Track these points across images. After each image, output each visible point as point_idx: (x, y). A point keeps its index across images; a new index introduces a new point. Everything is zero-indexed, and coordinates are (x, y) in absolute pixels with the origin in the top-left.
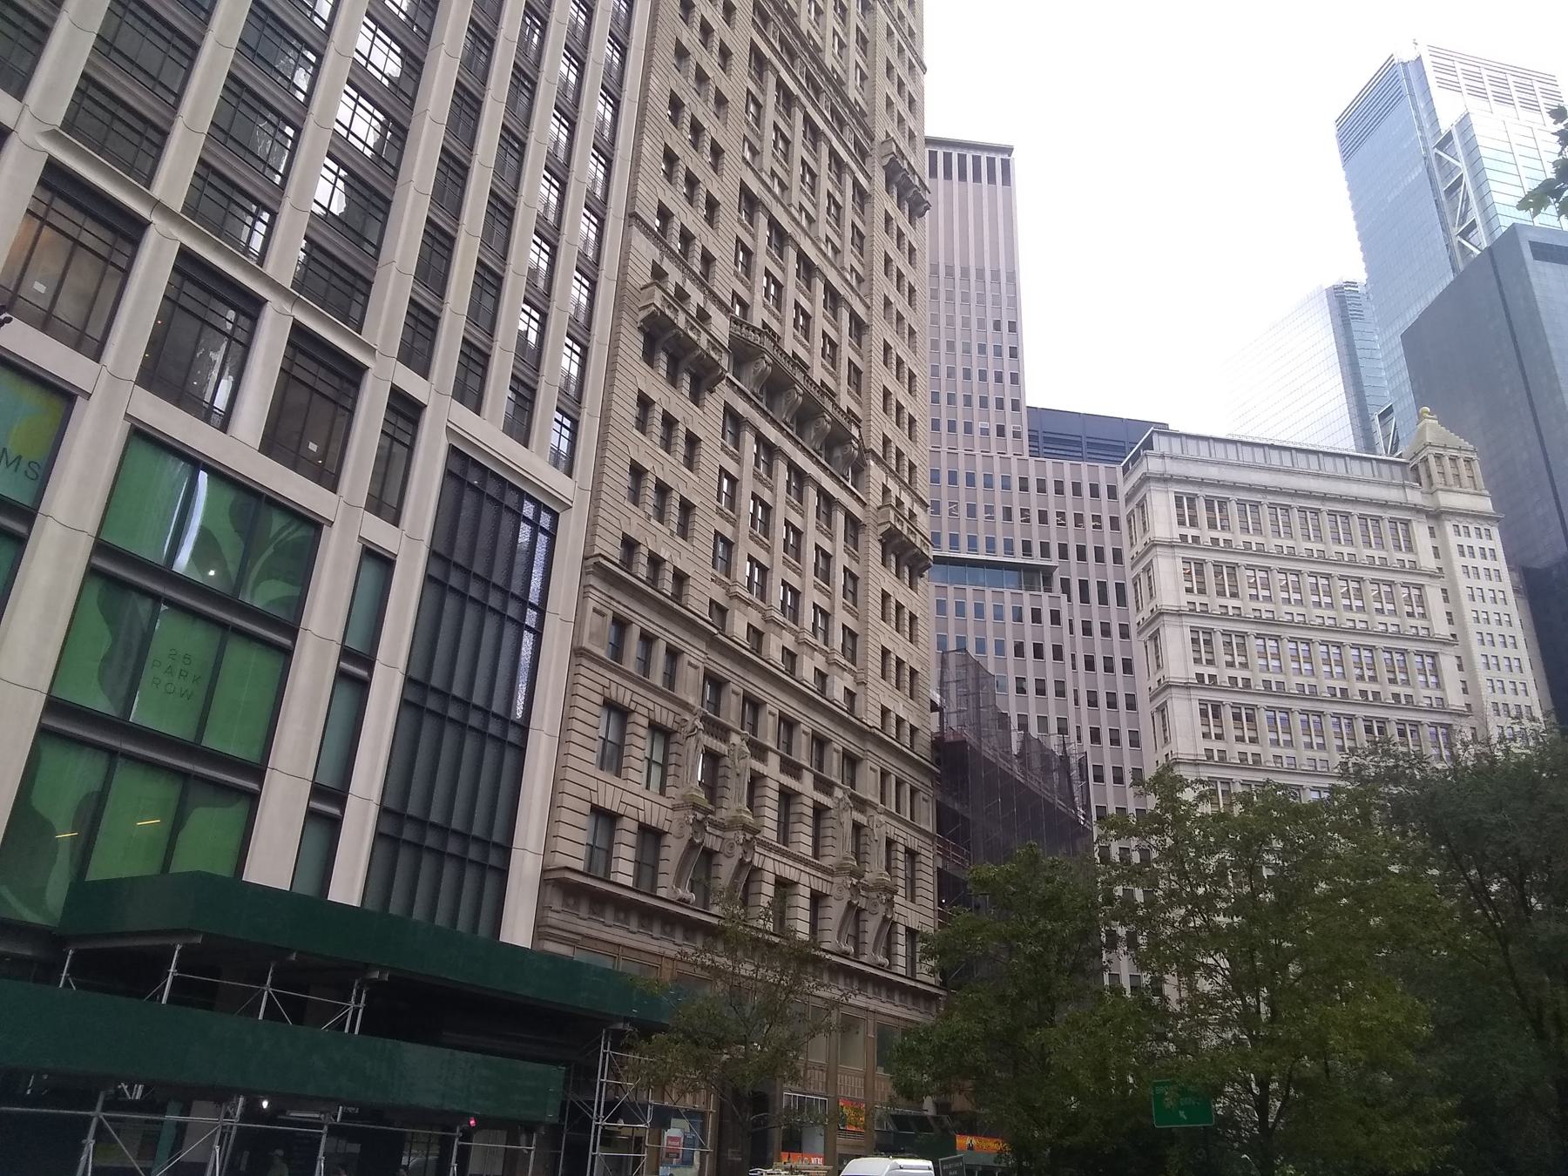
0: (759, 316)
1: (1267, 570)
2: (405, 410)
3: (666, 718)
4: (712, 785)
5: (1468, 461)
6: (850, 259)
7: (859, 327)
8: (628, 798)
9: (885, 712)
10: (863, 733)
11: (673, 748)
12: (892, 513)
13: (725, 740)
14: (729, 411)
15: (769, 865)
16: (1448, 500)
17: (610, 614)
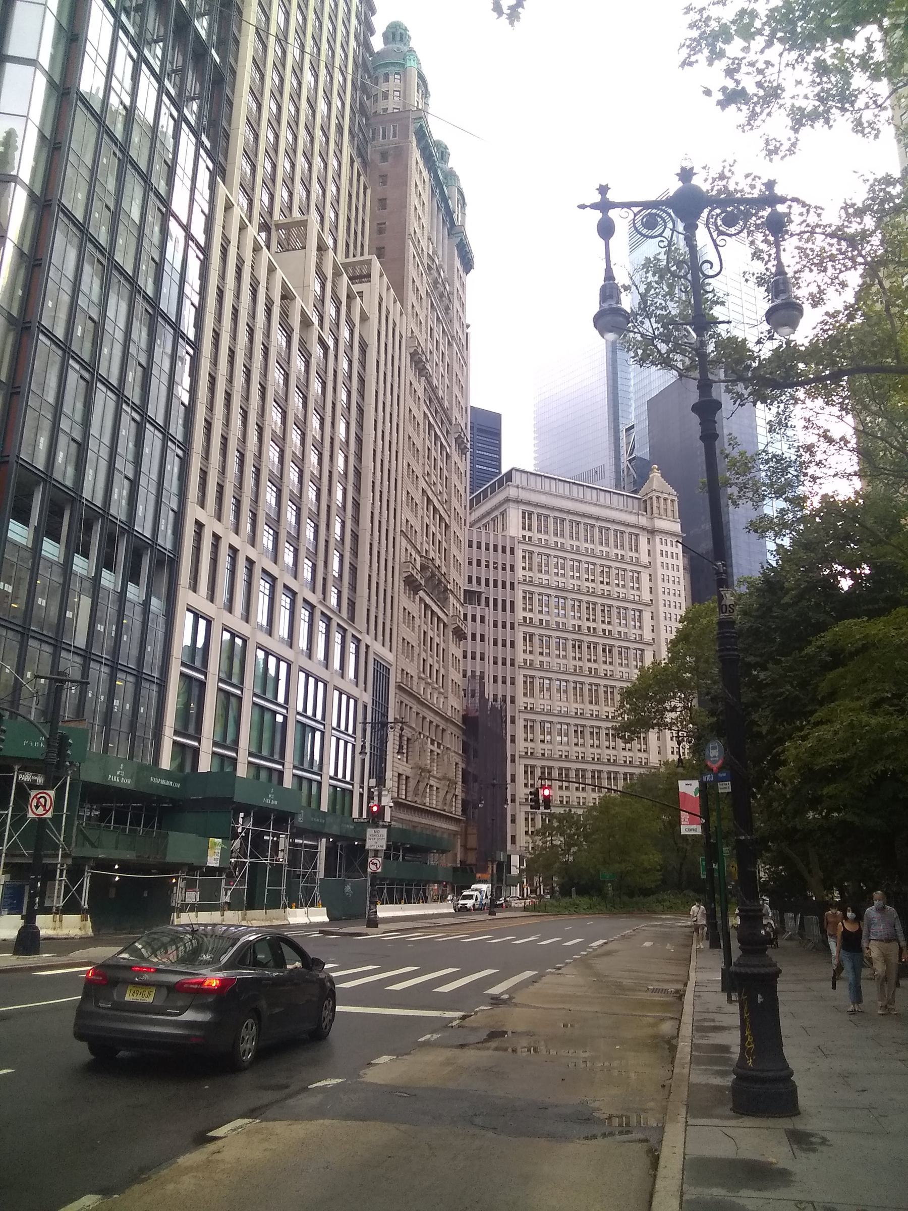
5: (672, 501)
16: (661, 524)
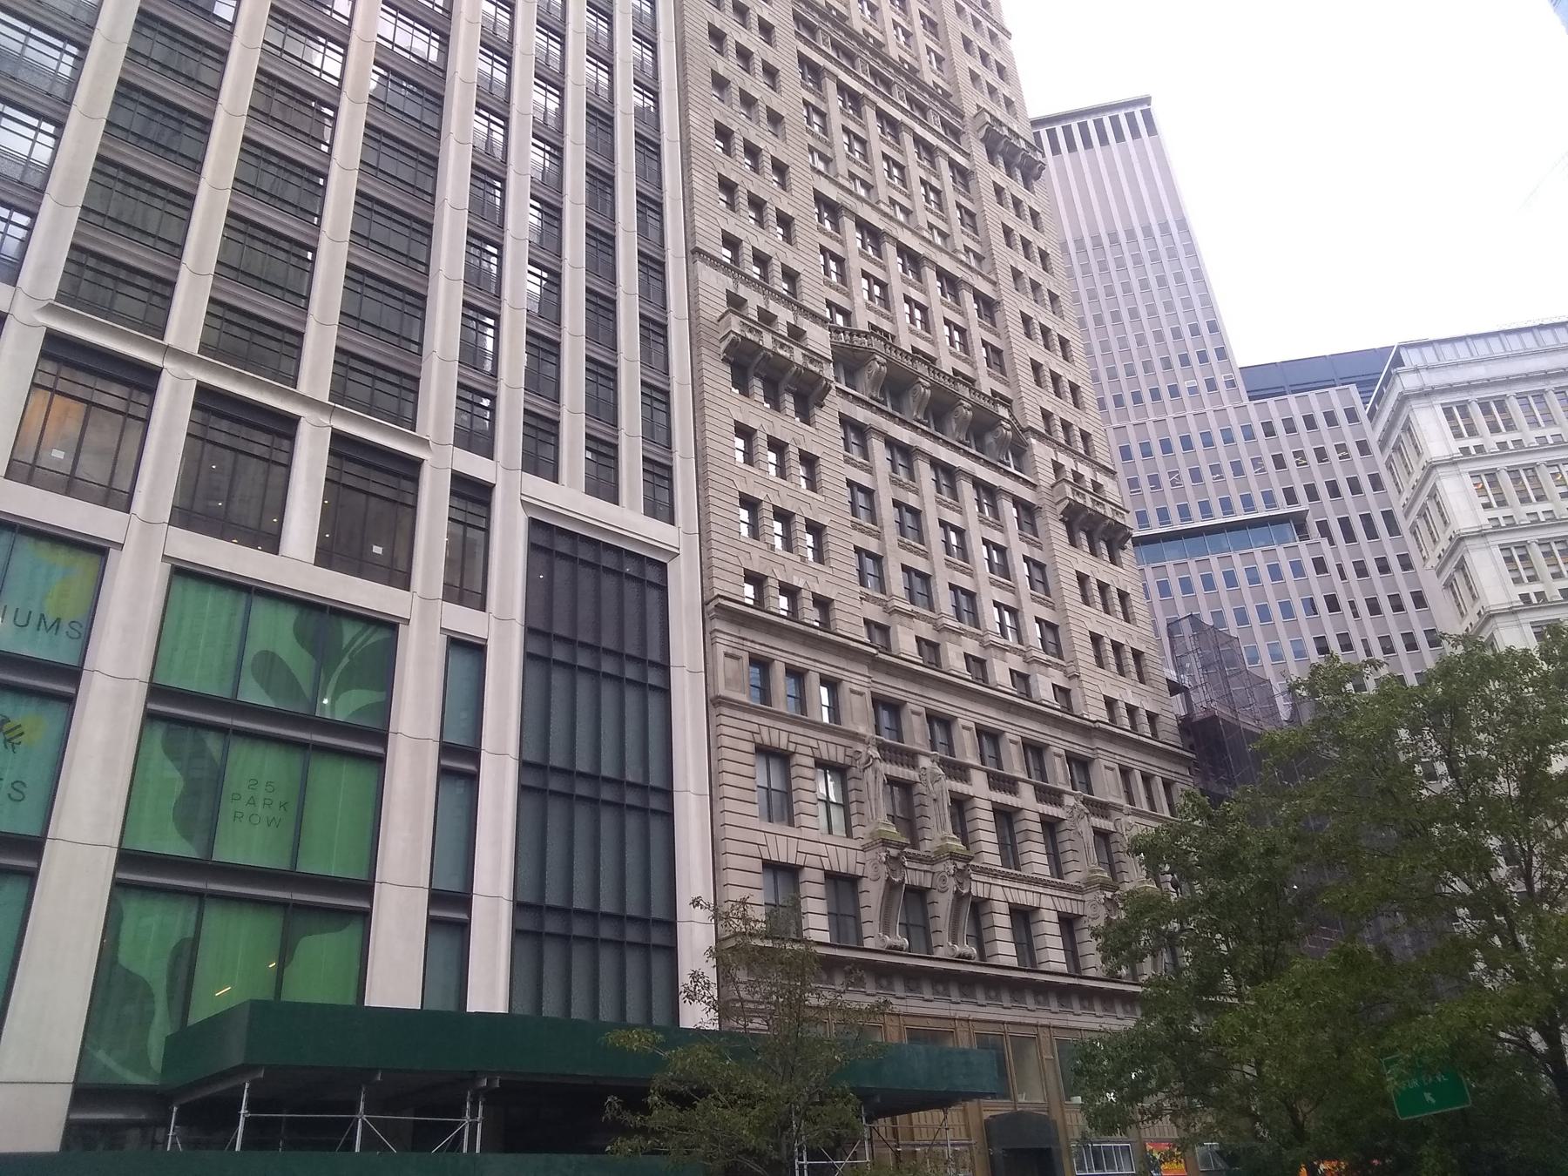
0: (863, 320)
2: (472, 496)
3: (836, 754)
4: (908, 819)
6: (961, 239)
7: (988, 306)
8: (805, 847)
9: (1110, 703)
10: (1087, 730)
11: (851, 784)
12: (1068, 488)
13: (913, 765)
14: (846, 422)
15: (997, 893)
17: (745, 656)
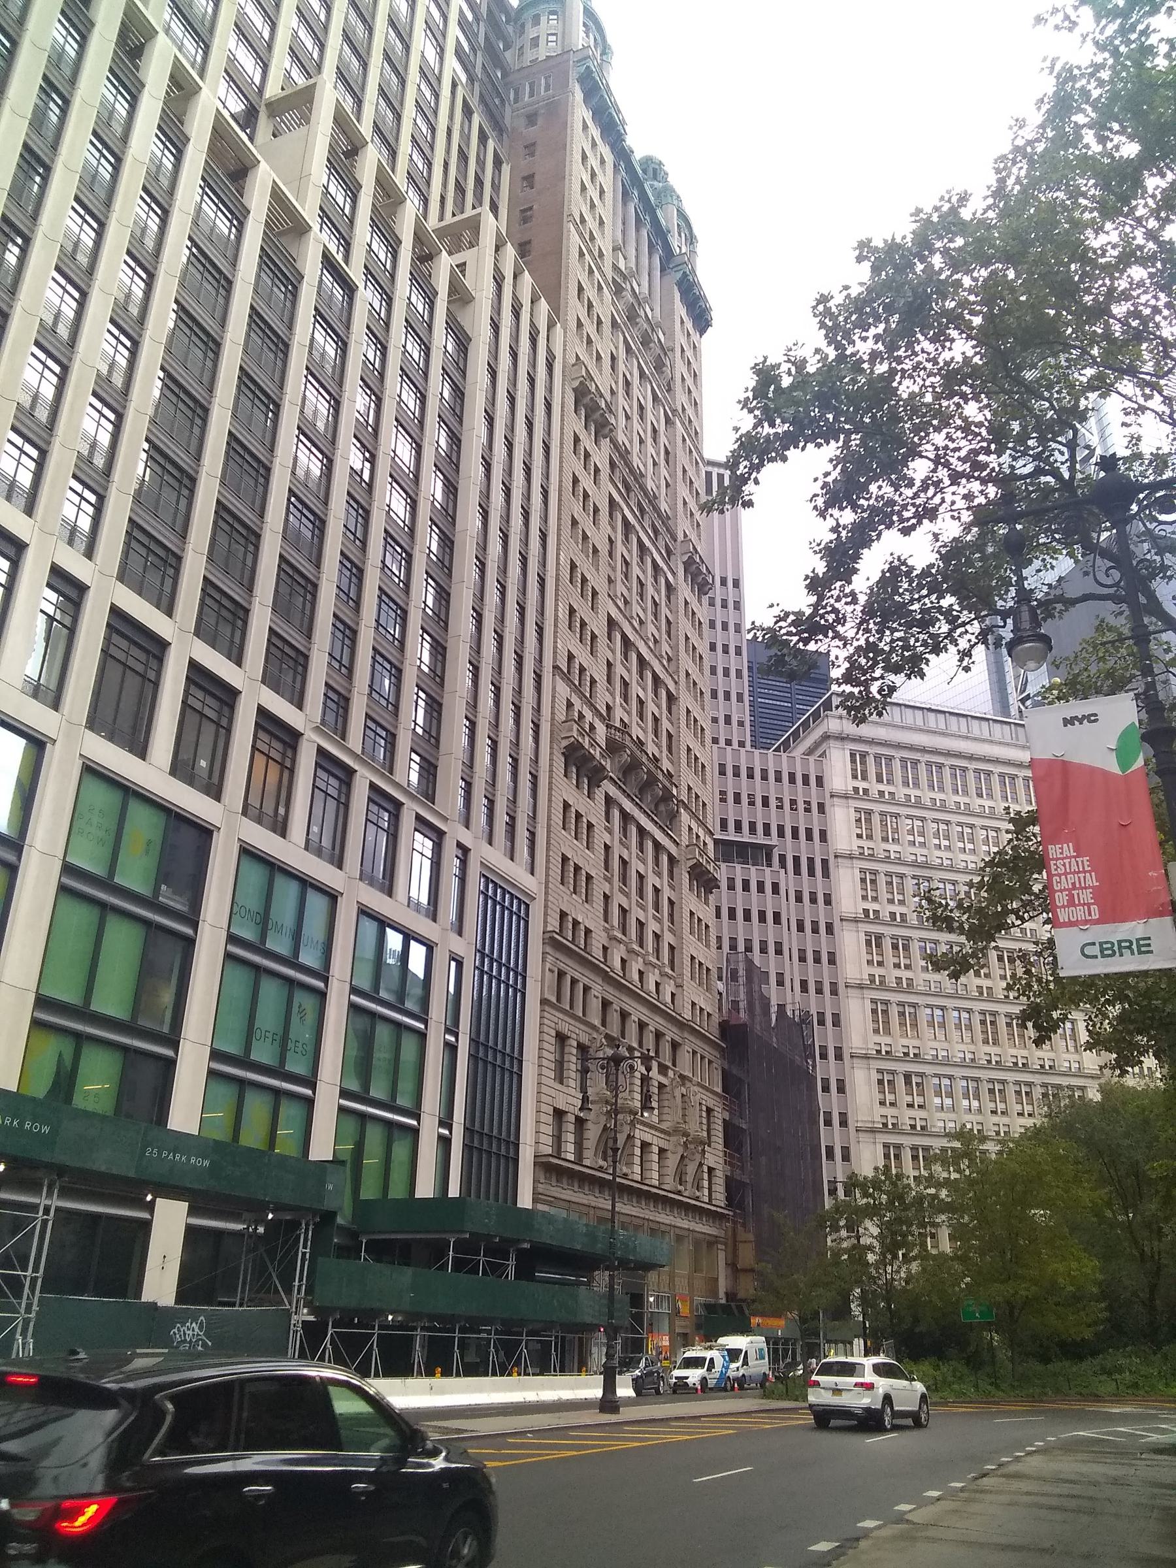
1: (923, 819)
